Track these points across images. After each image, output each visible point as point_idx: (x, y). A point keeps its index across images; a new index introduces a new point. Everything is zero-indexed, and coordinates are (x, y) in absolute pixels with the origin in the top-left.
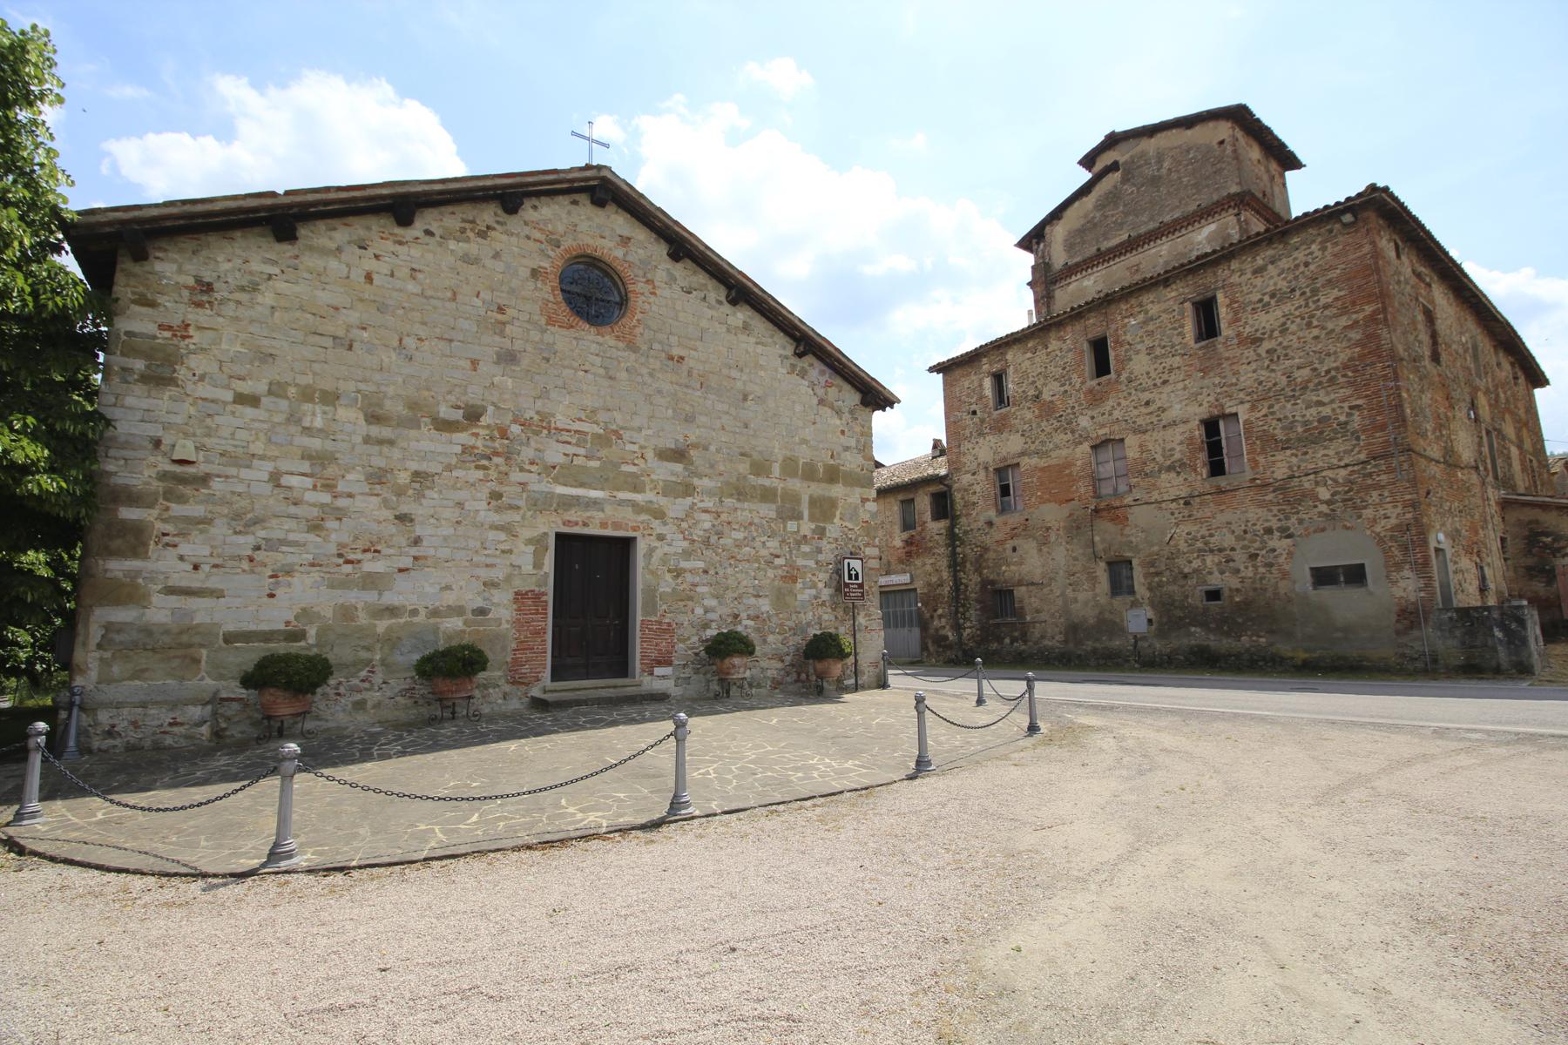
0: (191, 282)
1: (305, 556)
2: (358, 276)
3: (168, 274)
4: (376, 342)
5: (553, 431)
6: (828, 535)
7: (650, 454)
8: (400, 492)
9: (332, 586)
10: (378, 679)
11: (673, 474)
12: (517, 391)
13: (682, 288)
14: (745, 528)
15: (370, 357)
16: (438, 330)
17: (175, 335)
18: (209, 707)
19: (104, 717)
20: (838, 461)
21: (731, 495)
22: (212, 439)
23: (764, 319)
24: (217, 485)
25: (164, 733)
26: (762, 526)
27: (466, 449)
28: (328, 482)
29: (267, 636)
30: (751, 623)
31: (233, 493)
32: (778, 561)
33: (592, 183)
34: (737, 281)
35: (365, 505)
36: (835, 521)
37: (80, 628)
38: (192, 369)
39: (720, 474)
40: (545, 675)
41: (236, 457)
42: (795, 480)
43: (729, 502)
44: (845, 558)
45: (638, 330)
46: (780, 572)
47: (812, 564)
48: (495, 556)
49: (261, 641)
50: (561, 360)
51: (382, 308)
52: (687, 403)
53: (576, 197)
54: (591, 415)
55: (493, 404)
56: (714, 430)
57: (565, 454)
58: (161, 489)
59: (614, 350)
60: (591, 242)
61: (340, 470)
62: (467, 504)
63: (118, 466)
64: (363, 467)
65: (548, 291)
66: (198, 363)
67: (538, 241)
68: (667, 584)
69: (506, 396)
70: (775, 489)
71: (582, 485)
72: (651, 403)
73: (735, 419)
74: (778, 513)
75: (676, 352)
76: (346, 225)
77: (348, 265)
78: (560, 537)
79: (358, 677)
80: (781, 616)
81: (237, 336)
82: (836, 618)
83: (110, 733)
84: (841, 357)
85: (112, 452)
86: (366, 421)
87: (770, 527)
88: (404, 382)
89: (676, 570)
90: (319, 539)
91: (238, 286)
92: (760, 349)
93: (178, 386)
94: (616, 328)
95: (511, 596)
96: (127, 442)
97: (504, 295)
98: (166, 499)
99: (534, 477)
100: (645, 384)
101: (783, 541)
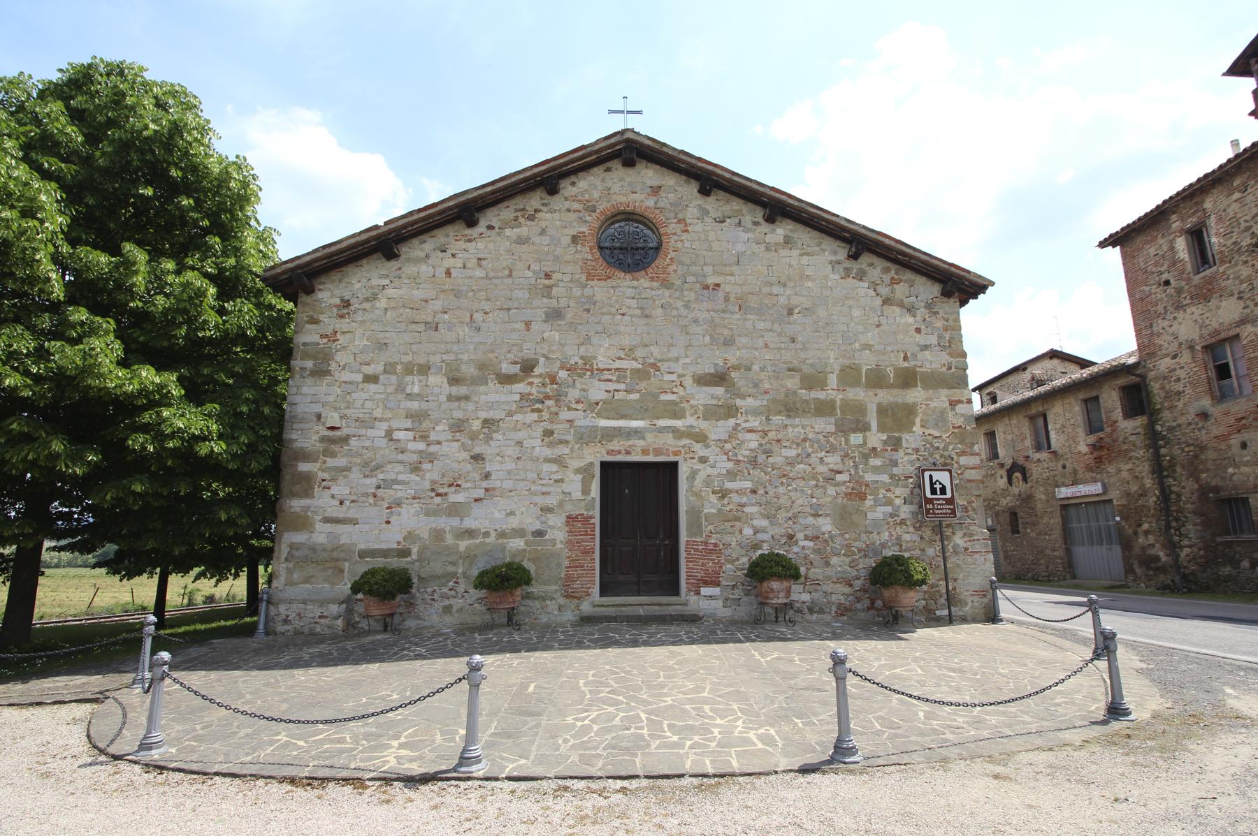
0: (338, 301)
2: (440, 273)
6: (904, 445)
7: (688, 381)
8: (474, 437)
9: (427, 515)
10: (461, 588)
11: (713, 397)
12: (563, 342)
13: (715, 219)
14: (798, 444)
16: (498, 303)
18: (344, 606)
19: (282, 609)
20: (914, 363)
21: (779, 413)
23: (808, 229)
24: (354, 442)
26: (818, 441)
27: (524, 397)
29: (385, 553)
30: (811, 544)
32: (839, 478)
33: (618, 147)
34: (771, 198)
36: (914, 429)
39: (766, 393)
42: (858, 389)
43: (777, 419)
44: (924, 471)
45: (671, 269)
47: (885, 478)
48: (550, 485)
51: (457, 294)
52: (725, 327)
54: (630, 353)
55: (544, 356)
56: (756, 349)
57: (607, 391)
59: (649, 291)
60: (623, 199)
64: (448, 419)
65: (586, 252)
66: (341, 357)
68: (711, 505)
69: (555, 348)
70: (833, 402)
71: (623, 417)
72: (687, 333)
73: (780, 335)
75: (711, 281)
77: (434, 267)
78: (605, 466)
82: (922, 538)
84: (904, 248)
85: (295, 426)
87: (828, 442)
90: (418, 478)
92: (805, 260)
94: (650, 270)
95: (564, 519)
98: (324, 456)
99: (581, 413)
101: (846, 455)
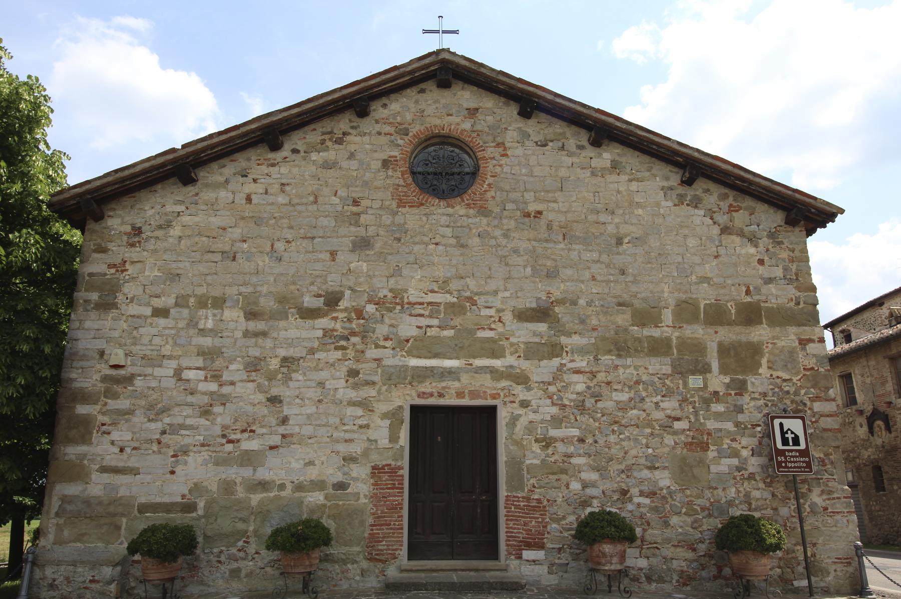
0: (128, 229)
1: (197, 437)
2: (240, 199)
3: (115, 226)
4: (254, 250)
5: (406, 306)
6: (750, 388)
7: (508, 317)
8: (271, 377)
9: (217, 464)
10: (252, 549)
11: (535, 334)
12: (371, 273)
13: (536, 143)
14: (630, 387)
15: (248, 264)
16: (302, 231)
17: (117, 271)
18: (119, 568)
19: (49, 571)
20: (756, 298)
21: (609, 352)
22: (138, 347)
23: (638, 153)
24: (139, 382)
25: (86, 588)
26: (653, 384)
27: (327, 333)
28: (216, 373)
29: (168, 508)
30: (647, 501)
31: (149, 388)
32: (677, 425)
33: (432, 68)
34: (596, 120)
35: (243, 390)
36: (760, 371)
37: (46, 498)
38: (126, 295)
39: (594, 330)
40: (401, 553)
41: (152, 359)
42: (696, 327)
43: (606, 359)
44: (773, 418)
45: (489, 195)
46: (683, 438)
47: (729, 426)
48: (353, 431)
49: (163, 512)
50: (412, 237)
51: (258, 221)
52: (548, 258)
53: (423, 86)
54: (444, 285)
55: (350, 288)
56: (582, 282)
57: (419, 327)
58: (103, 389)
59: (465, 218)
60: (438, 122)
61: (225, 362)
62: (327, 383)
63: (78, 374)
64: (243, 357)
65: (397, 177)
66: (130, 289)
67: (388, 134)
68: (534, 456)
69: (362, 280)
70: (668, 340)
71: (436, 356)
72: (507, 264)
73: (608, 266)
74: (673, 366)
75: (532, 208)
76: (232, 161)
77: (233, 193)
78: (414, 409)
79: (236, 546)
80: (688, 492)
81: (156, 264)
82: (773, 495)
83: (52, 586)
84: (742, 173)
85: (75, 364)
86: (245, 318)
87: (664, 385)
88: (275, 280)
89: (544, 440)
90: (208, 423)
91: (157, 226)
92: (634, 186)
93: (117, 308)
94: (466, 197)
95: (368, 470)
96: (84, 355)
97: (358, 189)
98: (105, 397)
99: (389, 352)
100: (500, 246)
101: (685, 400)
